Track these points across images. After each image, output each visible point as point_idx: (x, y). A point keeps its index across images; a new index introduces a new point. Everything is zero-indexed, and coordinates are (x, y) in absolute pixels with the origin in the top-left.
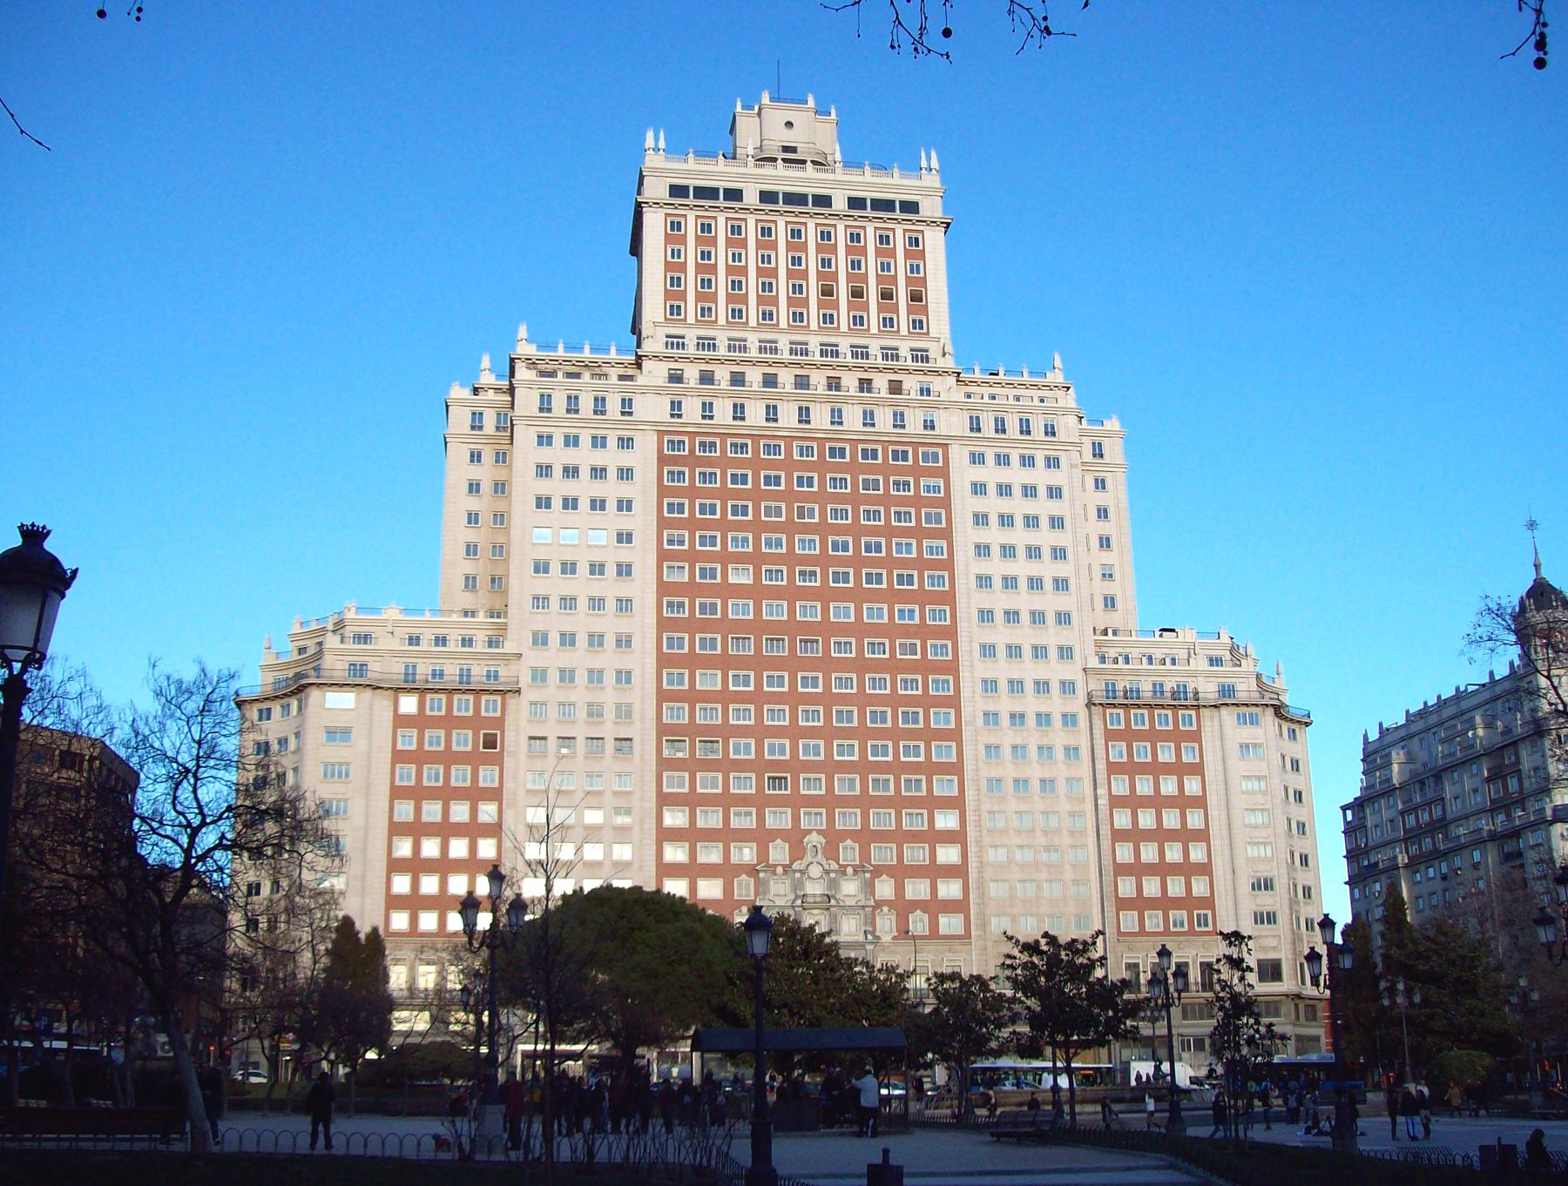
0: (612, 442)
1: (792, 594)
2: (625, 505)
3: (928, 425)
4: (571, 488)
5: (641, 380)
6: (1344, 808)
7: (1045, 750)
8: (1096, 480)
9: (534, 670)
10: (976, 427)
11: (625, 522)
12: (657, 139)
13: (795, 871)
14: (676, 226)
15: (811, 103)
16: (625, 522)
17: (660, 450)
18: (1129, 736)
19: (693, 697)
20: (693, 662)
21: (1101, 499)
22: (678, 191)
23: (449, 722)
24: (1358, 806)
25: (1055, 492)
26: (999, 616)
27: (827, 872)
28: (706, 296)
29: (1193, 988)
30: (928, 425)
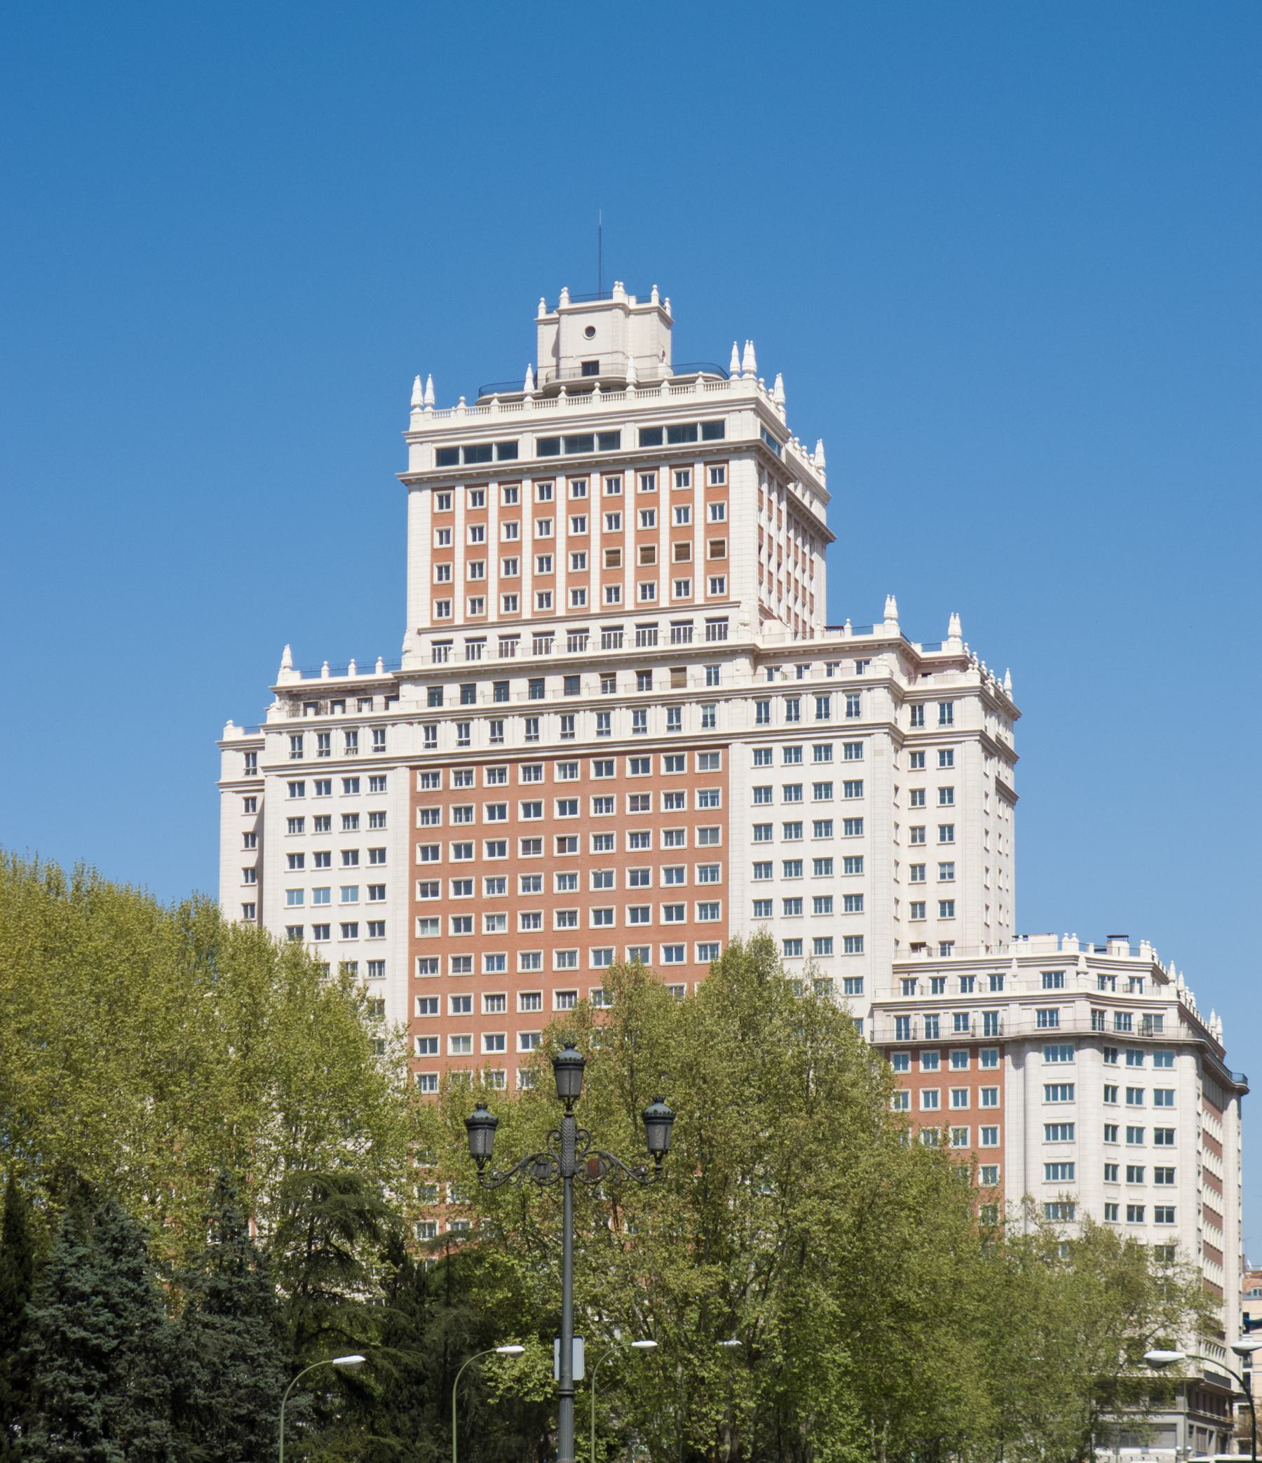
2: (378, 855)
3: (709, 721)
4: (323, 842)
8: (942, 753)
10: (763, 715)
11: (377, 875)
12: (424, 391)
14: (445, 501)
15: (619, 294)
17: (413, 787)
22: (446, 456)
30: (709, 721)
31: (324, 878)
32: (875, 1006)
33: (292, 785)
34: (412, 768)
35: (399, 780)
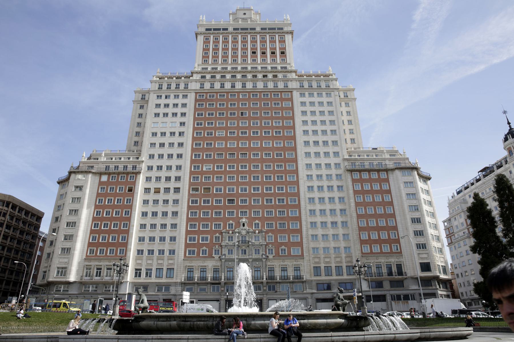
0: (181, 96)
1: (238, 139)
2: (183, 114)
3: (286, 86)
4: (166, 110)
5: (191, 78)
6: (444, 222)
7: (330, 188)
8: (346, 103)
9: (149, 167)
11: (183, 120)
12: (203, 17)
13: (236, 232)
16: (183, 120)
18: (361, 181)
19: (202, 173)
20: (203, 162)
21: (348, 109)
23: (118, 183)
24: (449, 220)
25: (330, 104)
26: (311, 143)
27: (248, 232)
28: (215, 57)
29: (394, 274)
31: (165, 119)
32: (345, 160)
33: (158, 96)
34: (196, 93)
35: (192, 96)
